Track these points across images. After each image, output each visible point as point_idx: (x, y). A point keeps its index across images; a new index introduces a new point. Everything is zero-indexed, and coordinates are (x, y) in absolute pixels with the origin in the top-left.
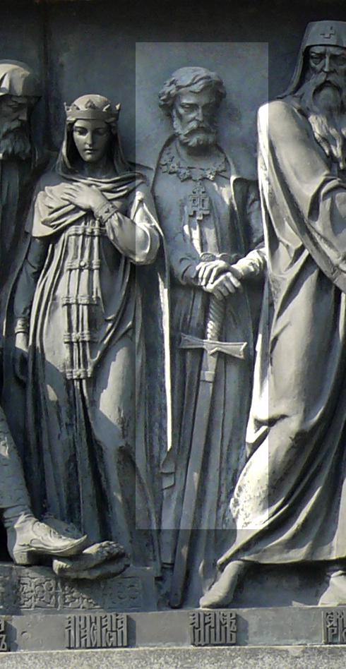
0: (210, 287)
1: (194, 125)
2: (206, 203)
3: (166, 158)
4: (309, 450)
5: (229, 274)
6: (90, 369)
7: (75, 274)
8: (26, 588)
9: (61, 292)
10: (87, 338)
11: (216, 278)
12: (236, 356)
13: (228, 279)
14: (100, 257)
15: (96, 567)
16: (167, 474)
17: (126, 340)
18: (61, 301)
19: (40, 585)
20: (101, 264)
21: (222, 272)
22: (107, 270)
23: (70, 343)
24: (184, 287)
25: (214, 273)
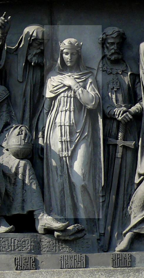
0: (120, 118)
1: (113, 51)
2: (118, 84)
5: (127, 113)
6: (70, 152)
7: (64, 113)
8: (43, 244)
9: (58, 120)
10: (68, 140)
11: (122, 115)
12: (131, 147)
13: (127, 115)
14: (74, 106)
15: (72, 235)
17: (85, 140)
18: (58, 124)
19: (49, 242)
20: (74, 109)
21: (124, 112)
22: (77, 111)
23: (62, 142)
24: (108, 118)
25: (121, 113)
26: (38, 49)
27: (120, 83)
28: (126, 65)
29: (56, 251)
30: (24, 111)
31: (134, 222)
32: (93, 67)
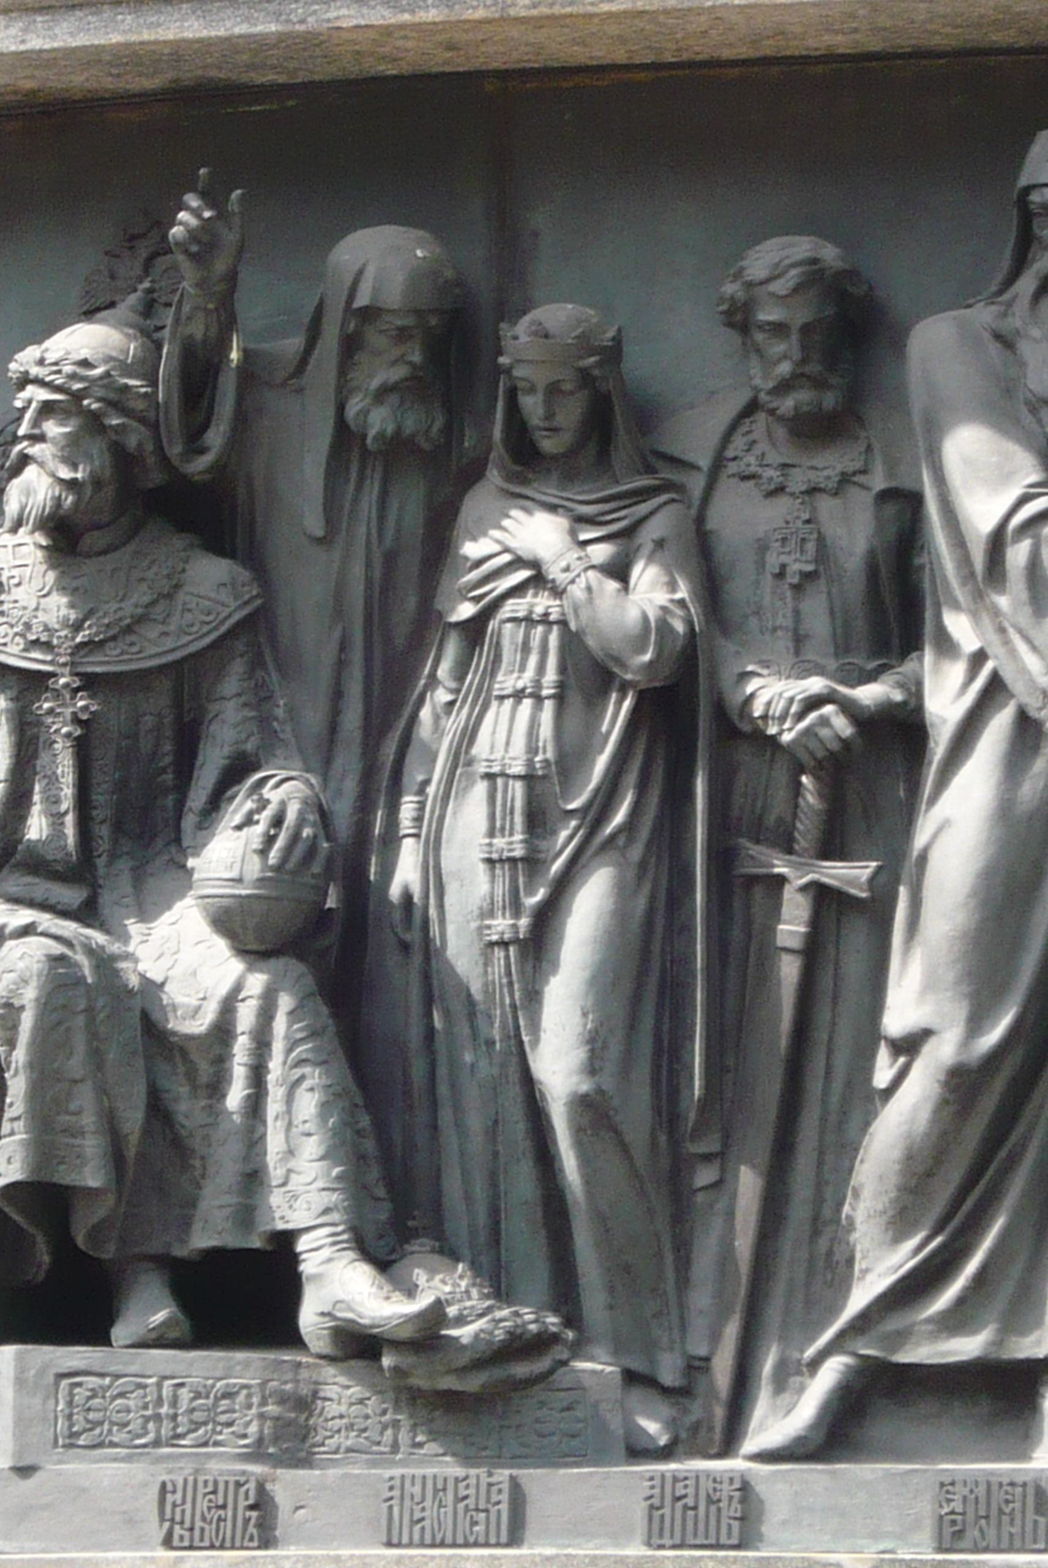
1: (785, 368)
2: (811, 547)
3: (739, 442)
4: (989, 1103)
5: (828, 709)
6: (524, 922)
8: (332, 1409)
12: (853, 891)
13: (824, 721)
14: (562, 669)
16: (707, 1158)
17: (614, 855)
19: (361, 1402)
20: (561, 685)
22: (575, 699)
23: (490, 861)
26: (394, 363)
27: (821, 540)
28: (869, 449)
29: (395, 1447)
30: (337, 695)
31: (860, 1298)
32: (689, 457)
